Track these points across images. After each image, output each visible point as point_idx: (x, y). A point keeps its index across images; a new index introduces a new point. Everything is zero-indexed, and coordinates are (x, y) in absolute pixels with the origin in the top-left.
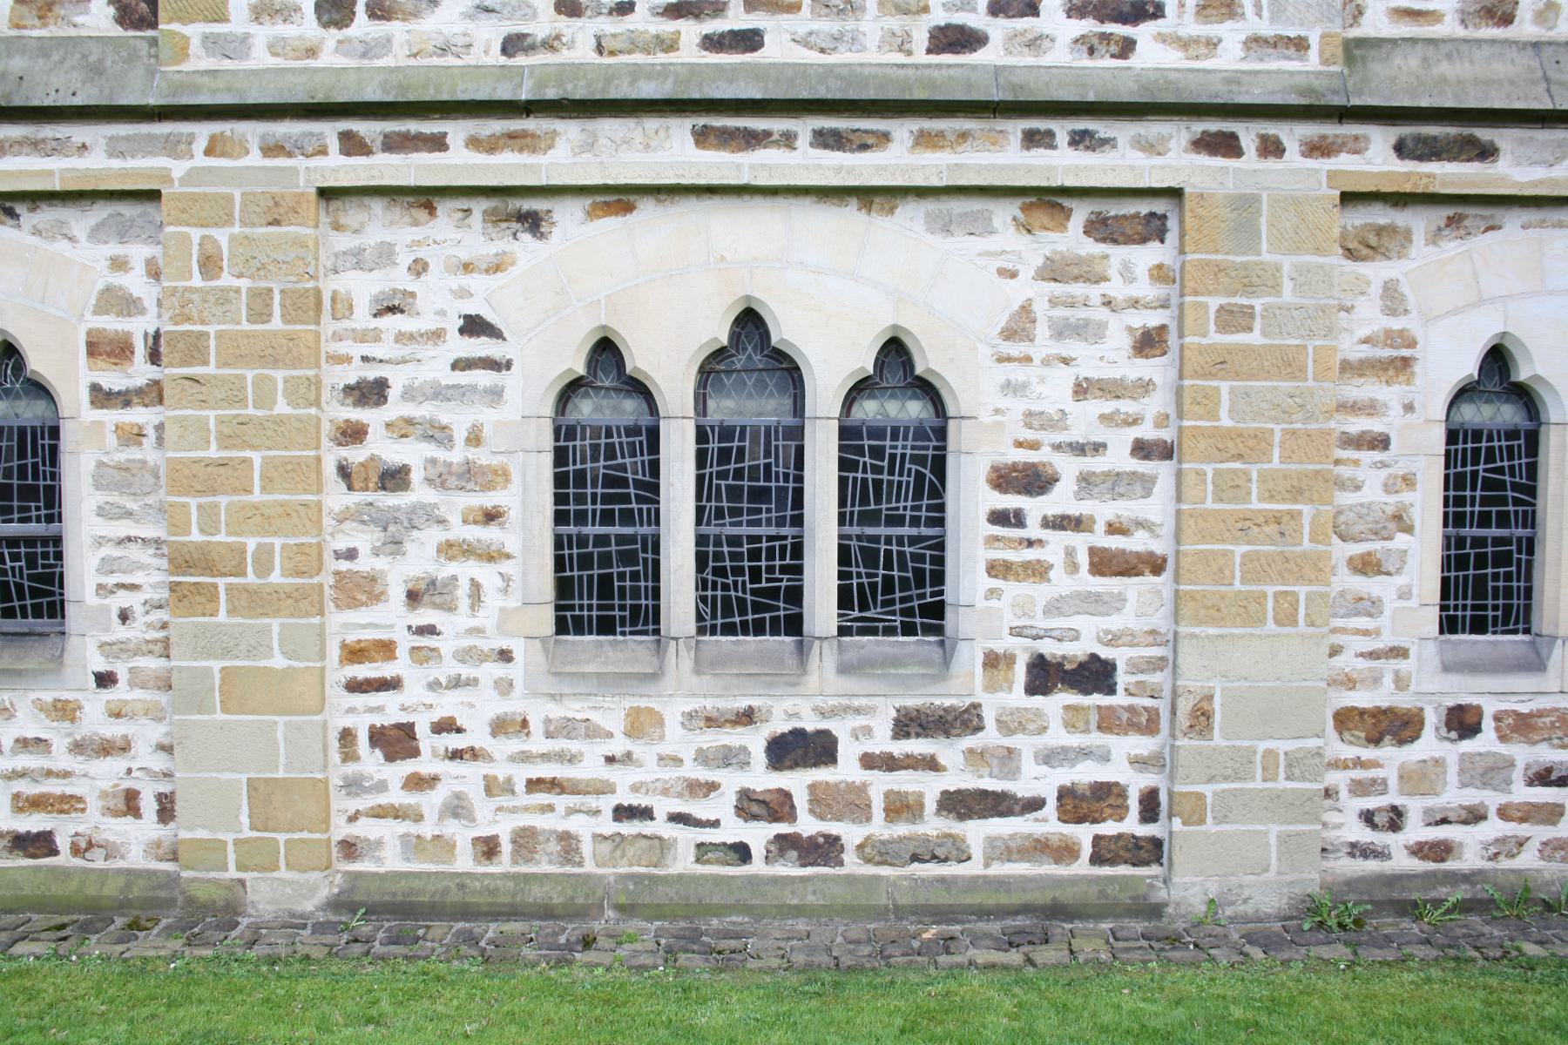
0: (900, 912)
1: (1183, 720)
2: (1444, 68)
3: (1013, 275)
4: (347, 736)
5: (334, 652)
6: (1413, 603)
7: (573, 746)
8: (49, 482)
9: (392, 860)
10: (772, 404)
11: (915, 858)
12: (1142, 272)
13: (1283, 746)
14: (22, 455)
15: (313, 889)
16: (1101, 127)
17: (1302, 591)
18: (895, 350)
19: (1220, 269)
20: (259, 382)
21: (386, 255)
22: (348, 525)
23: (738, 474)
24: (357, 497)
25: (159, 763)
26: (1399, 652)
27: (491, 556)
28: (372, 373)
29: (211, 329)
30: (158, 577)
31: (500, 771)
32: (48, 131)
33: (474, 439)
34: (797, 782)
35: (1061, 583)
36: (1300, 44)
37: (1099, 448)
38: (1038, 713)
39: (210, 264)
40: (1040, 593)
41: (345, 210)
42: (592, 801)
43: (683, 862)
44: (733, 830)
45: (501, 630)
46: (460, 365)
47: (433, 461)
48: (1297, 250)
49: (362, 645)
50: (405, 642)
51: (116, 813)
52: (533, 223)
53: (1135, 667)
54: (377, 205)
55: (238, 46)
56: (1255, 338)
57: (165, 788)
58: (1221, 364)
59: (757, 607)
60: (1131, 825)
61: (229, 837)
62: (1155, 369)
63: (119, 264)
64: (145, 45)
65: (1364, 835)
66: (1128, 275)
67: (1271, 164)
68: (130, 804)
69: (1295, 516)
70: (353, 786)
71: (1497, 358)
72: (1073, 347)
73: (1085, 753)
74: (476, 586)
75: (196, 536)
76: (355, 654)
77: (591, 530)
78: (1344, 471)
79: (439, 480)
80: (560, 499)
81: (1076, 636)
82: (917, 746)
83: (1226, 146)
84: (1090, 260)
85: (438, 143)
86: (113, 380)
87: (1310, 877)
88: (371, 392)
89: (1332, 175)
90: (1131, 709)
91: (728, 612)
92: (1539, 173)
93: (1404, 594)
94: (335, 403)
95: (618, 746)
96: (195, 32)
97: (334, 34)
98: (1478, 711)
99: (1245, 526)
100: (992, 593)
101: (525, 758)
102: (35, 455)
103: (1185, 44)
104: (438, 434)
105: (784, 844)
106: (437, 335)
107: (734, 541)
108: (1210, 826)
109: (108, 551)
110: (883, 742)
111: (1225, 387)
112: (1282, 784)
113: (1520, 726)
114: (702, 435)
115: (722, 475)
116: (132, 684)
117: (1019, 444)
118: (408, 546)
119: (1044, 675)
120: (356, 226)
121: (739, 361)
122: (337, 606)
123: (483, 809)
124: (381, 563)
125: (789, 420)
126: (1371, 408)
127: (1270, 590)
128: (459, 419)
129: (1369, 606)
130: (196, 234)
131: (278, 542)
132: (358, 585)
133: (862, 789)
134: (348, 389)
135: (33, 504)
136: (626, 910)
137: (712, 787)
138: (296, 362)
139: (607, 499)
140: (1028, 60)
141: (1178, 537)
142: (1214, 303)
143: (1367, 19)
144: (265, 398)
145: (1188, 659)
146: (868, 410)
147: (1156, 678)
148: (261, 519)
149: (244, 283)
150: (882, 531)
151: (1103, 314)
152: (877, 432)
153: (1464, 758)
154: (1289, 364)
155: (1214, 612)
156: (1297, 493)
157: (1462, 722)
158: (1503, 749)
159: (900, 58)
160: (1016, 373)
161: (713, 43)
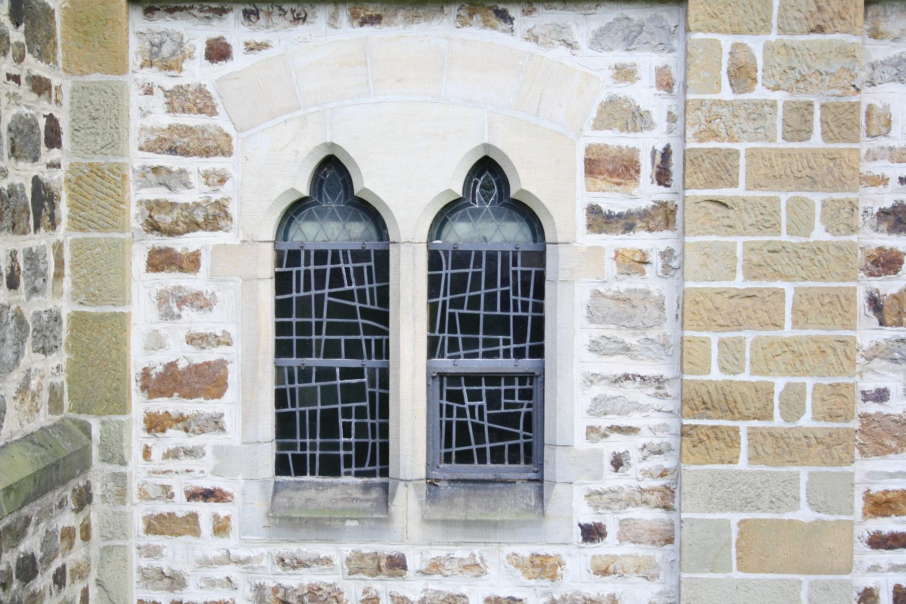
5: (859, 504)
8: (520, 313)
14: (491, 282)
20: (795, 206)
22: (876, 363)
29: (741, 147)
30: (657, 420)
41: (885, 16)
49: (889, 496)
63: (625, 73)
75: (716, 375)
94: (868, 230)
102: (505, 282)
109: (599, 390)
116: (622, 538)
120: (896, 33)
122: (862, 453)
130: (726, 41)
131: (810, 382)
132: (888, 430)
134: (883, 214)
135: (501, 337)
138: (840, 184)
149: (780, 97)
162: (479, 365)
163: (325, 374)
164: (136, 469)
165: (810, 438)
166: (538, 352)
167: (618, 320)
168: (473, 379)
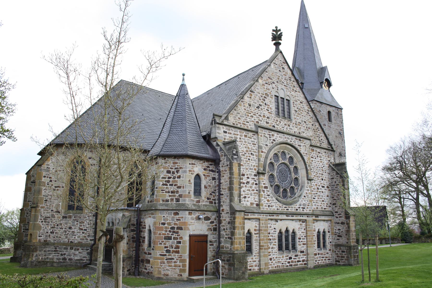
27: (275, 245)
31: (276, 261)
34: (290, 260)
43: (285, 267)
46: (274, 231)
50: (271, 252)
52: (277, 221)
58: (309, 231)
68: (256, 266)
85: (274, 216)
88: (269, 233)
95: (282, 259)
96: (262, 207)
101: (277, 260)
104: (272, 236)
113: (321, 254)
128: (274, 235)
141: (307, 242)
155: (310, 247)
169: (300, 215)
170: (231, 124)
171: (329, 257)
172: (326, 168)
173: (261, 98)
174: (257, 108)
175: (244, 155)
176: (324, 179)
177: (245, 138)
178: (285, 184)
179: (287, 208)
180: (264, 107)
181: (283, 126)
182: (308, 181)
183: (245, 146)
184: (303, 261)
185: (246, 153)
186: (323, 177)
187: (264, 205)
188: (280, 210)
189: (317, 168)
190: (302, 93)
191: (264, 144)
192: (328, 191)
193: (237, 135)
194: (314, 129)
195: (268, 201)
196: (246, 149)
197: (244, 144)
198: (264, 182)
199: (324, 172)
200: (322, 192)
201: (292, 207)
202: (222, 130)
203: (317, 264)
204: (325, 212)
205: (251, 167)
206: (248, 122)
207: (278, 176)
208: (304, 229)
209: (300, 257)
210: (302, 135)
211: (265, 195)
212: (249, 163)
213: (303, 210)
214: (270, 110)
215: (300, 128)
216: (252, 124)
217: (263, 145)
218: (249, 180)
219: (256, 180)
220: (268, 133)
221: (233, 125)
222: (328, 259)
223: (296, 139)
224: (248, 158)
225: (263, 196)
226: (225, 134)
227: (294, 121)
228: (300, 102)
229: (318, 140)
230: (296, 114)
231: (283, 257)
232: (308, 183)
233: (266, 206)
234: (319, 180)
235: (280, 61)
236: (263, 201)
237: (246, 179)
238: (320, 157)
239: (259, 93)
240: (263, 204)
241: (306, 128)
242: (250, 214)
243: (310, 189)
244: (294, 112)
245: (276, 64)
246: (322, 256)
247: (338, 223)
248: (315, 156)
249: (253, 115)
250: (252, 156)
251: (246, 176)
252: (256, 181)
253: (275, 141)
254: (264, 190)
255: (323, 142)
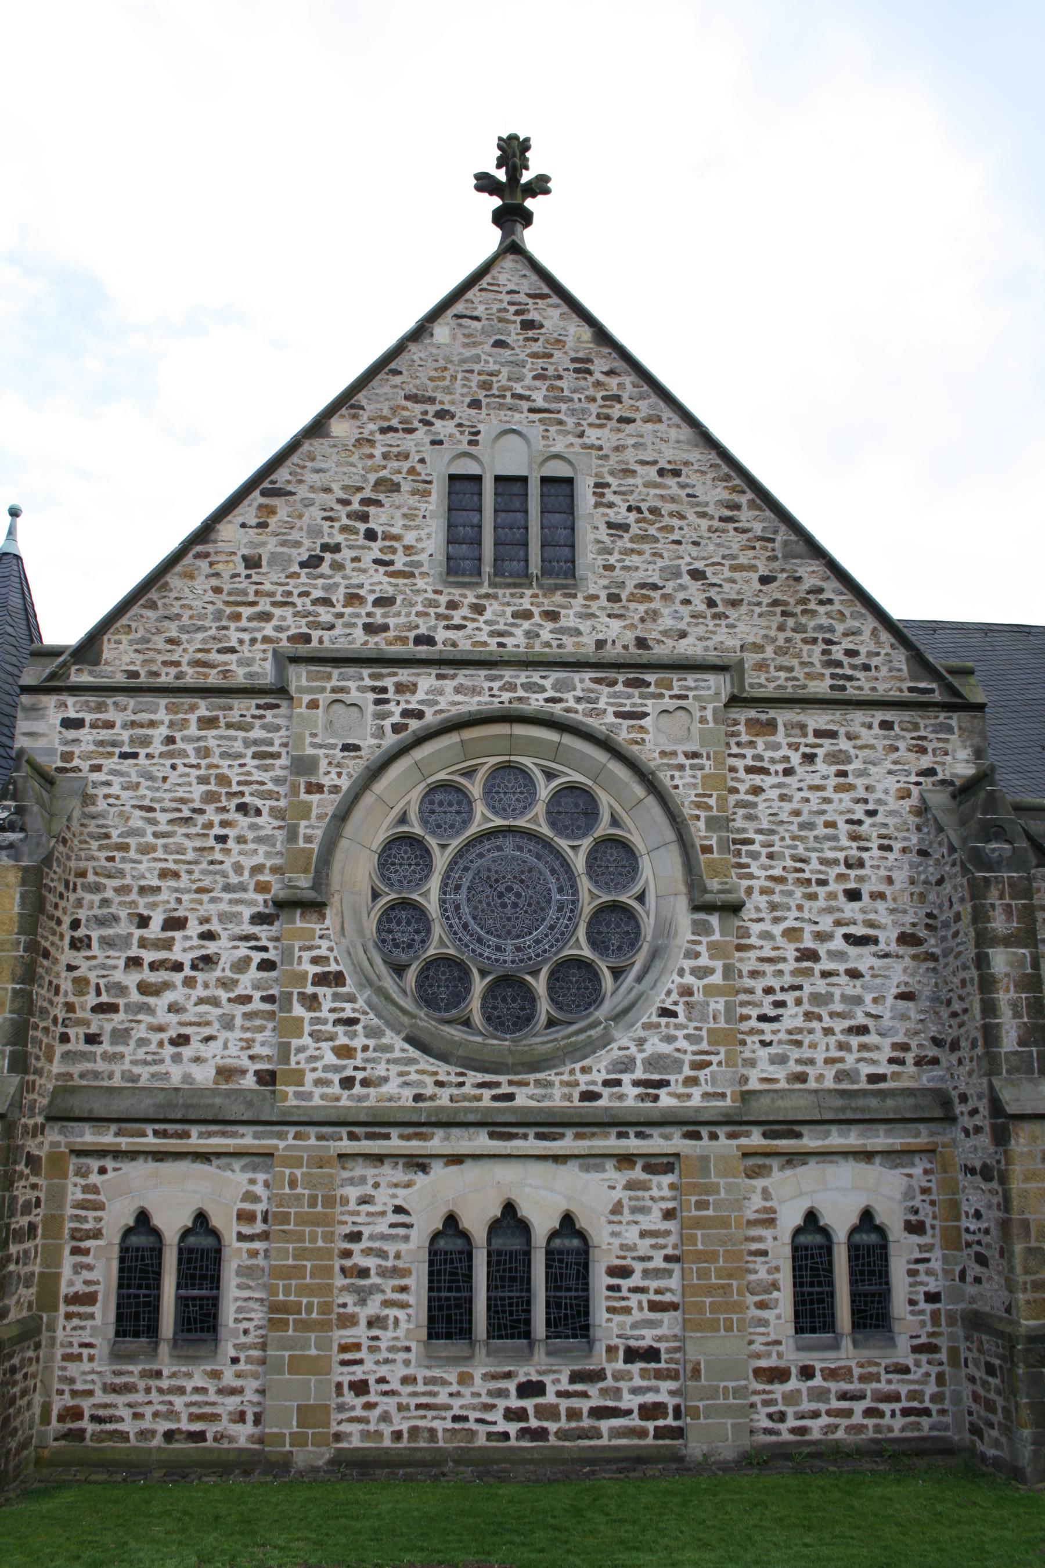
0: (573, 1461)
1: (689, 1374)
2: (780, 1103)
3: (614, 1188)
4: (339, 1385)
5: (335, 1348)
6: (782, 1321)
7: (436, 1389)
9: (356, 1442)
10: (517, 1241)
11: (580, 1437)
12: (665, 1186)
13: (731, 1384)
15: (323, 1455)
16: (647, 1130)
17: (735, 1317)
18: (568, 1219)
19: (695, 1185)
20: (311, 1233)
21: (363, 1180)
23: (504, 1270)
24: (348, 1281)
25: (256, 1398)
26: (778, 1343)
27: (403, 1305)
28: (356, 1229)
29: (292, 1210)
30: (260, 1315)
31: (404, 1400)
32: (229, 1128)
33: (398, 1256)
34: (529, 1404)
35: (637, 1315)
36: (723, 1095)
37: (650, 1258)
38: (629, 1372)
39: (293, 1184)
40: (628, 1320)
42: (443, 1414)
43: (481, 1441)
44: (502, 1426)
45: (407, 1338)
46: (392, 1226)
47: (380, 1266)
48: (725, 1176)
51: (235, 1422)
52: (424, 1168)
53: (669, 1351)
54: (360, 1160)
55: (309, 1096)
56: (710, 1212)
57: (257, 1410)
58: (698, 1223)
59: (512, 1328)
60: (670, 1421)
61: (287, 1431)
62: (671, 1225)
63: (252, 1182)
64: (268, 1094)
65: (767, 1423)
66: (660, 1187)
67: (714, 1143)
68: (241, 1417)
69: (730, 1285)
70: (341, 1408)
71: (811, 1216)
72: (639, 1217)
73: (649, 1389)
74: (396, 1320)
75: (281, 1297)
76: (344, 1348)
77: (444, 1294)
78: (751, 1266)
79: (383, 1273)
80: (430, 1281)
81: (643, 1338)
82: (579, 1387)
83: (696, 1136)
84: (644, 1181)
85: (387, 1137)
86: (247, 1230)
87: (746, 1443)
88: (355, 1237)
89: (738, 1147)
90: (668, 1369)
91: (499, 1330)
92: (819, 1143)
93: (779, 1317)
95: (454, 1388)
96: (291, 1090)
97: (346, 1093)
98: (813, 1367)
99: (710, 1290)
100: (609, 1320)
101: (415, 1394)
103: (678, 1096)
104: (382, 1254)
105: (523, 1433)
106: (383, 1213)
107: (503, 1299)
108: (702, 1420)
109: (239, 1303)
110: (565, 1386)
111: (699, 1233)
112: (732, 1401)
113: (831, 1374)
114: (489, 1255)
115: (498, 1271)
116: (246, 1363)
117: (618, 1257)
118: (369, 1302)
119: (632, 1355)
121: (505, 1223)
123: (396, 1417)
124: (357, 1309)
125: (525, 1248)
126: (760, 1239)
127: (722, 1317)
128: (391, 1248)
129: (764, 1323)
130: (287, 1171)
131: (316, 1300)
133: (557, 1406)
134: (346, 1236)
136: (457, 1462)
137: (494, 1406)
139: (450, 1281)
140: (618, 1104)
142: (693, 1199)
143: (751, 1081)
144: (313, 1239)
145: (690, 1347)
146: (557, 1243)
147: (677, 1355)
148: (310, 1290)
149: (306, 1192)
150: (563, 1294)
151: (650, 1203)
152: (560, 1252)
153: (809, 1388)
154: (724, 1223)
155: (699, 1326)
156: (730, 1276)
157: (807, 1373)
158: (825, 1384)
159: (568, 1104)
160: (617, 1228)
161: (495, 1098)
162: (195, 1292)
163: (137, 1296)
164: (60, 1334)
165: (315, 1322)
166: (218, 1288)
167: (248, 1276)
168: (194, 1299)
169: (614, 1131)
170: (120, 679)
171: (913, 1395)
172: (889, 821)
173: (342, 511)
174: (303, 565)
175: (187, 821)
176: (866, 889)
177: (203, 733)
178: (518, 949)
179: (505, 1089)
180: (353, 554)
181: (501, 627)
182: (702, 916)
183: (195, 772)
184: (649, 1411)
185: (201, 812)
186: (860, 879)
187: (310, 1077)
188: (445, 1101)
189: (810, 826)
190: (676, 419)
191: (333, 746)
192: (907, 960)
193: (152, 724)
194: (775, 603)
195: (344, 1052)
196: (204, 788)
197: (197, 766)
198: (315, 953)
199: (874, 844)
200: (854, 974)
201: (549, 1084)
202: (55, 718)
203: (787, 1437)
204: (873, 1102)
205: (234, 879)
206: (232, 650)
207: (465, 910)
208: (669, 1215)
209: (623, 1385)
210: (661, 651)
211: (317, 1021)
212: (218, 856)
213: (641, 1098)
214: (400, 561)
215: (655, 615)
216: (261, 655)
217: (321, 752)
218: (211, 948)
219: (264, 943)
220: (368, 682)
221: (133, 682)
222: (906, 1412)
223: (597, 681)
224: (218, 830)
225: (307, 1028)
226: (71, 734)
227: (595, 584)
228: (661, 472)
229: (817, 658)
230: (625, 542)
231: (465, 1379)
232: (701, 928)
233: (318, 1082)
234: (821, 903)
235: (511, 292)
236: (302, 1057)
237: (196, 942)
238: (835, 757)
239: (327, 490)
240: (301, 1073)
241: (702, 607)
242: (203, 1128)
243: (718, 965)
244: (603, 533)
245: (477, 319)
246: (834, 1386)
247: (972, 1171)
248: (786, 759)
249: (268, 608)
250: (243, 821)
251: (194, 928)
252: (265, 949)
253: (419, 715)
254: (315, 996)
255: (866, 668)
